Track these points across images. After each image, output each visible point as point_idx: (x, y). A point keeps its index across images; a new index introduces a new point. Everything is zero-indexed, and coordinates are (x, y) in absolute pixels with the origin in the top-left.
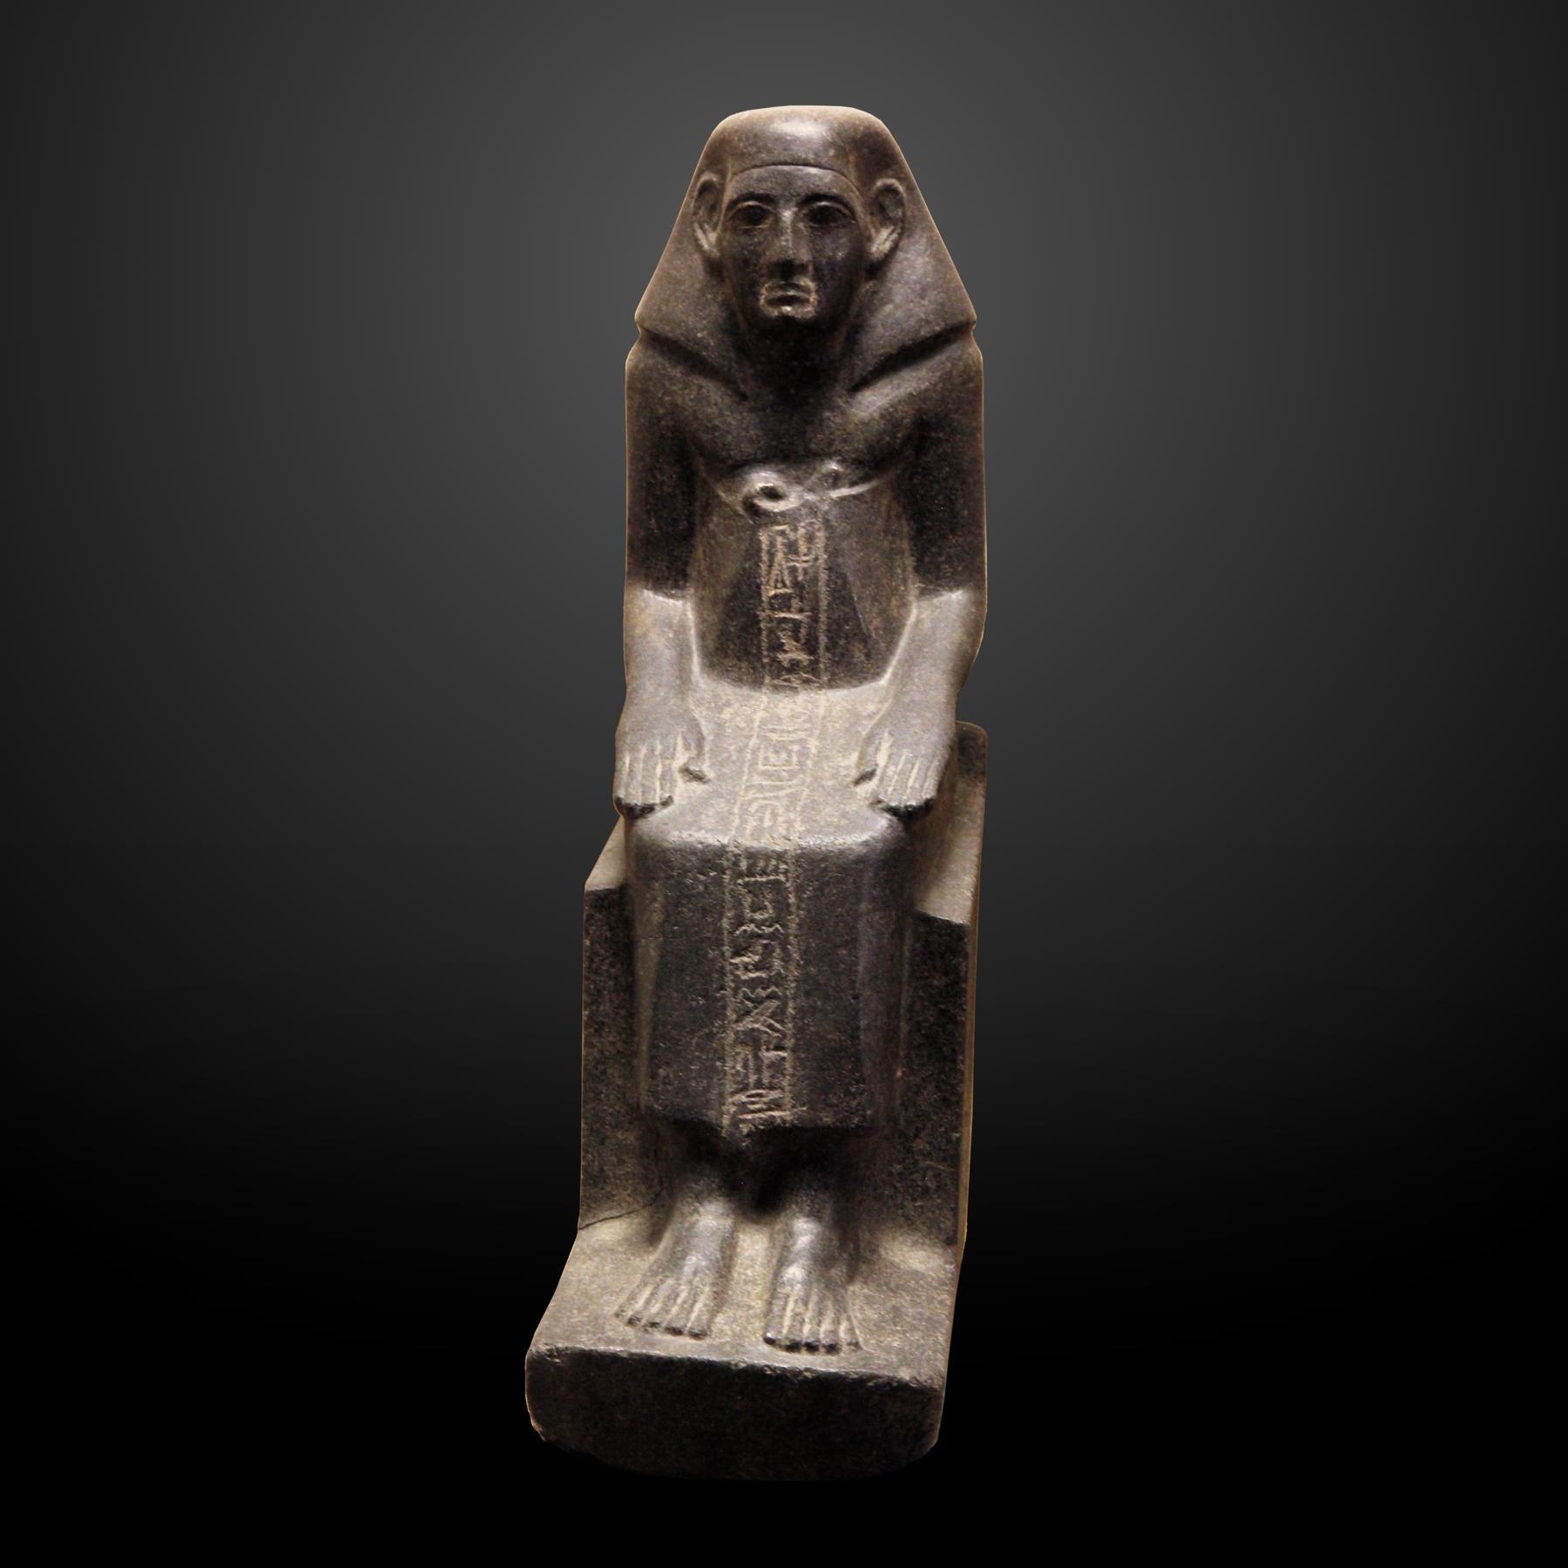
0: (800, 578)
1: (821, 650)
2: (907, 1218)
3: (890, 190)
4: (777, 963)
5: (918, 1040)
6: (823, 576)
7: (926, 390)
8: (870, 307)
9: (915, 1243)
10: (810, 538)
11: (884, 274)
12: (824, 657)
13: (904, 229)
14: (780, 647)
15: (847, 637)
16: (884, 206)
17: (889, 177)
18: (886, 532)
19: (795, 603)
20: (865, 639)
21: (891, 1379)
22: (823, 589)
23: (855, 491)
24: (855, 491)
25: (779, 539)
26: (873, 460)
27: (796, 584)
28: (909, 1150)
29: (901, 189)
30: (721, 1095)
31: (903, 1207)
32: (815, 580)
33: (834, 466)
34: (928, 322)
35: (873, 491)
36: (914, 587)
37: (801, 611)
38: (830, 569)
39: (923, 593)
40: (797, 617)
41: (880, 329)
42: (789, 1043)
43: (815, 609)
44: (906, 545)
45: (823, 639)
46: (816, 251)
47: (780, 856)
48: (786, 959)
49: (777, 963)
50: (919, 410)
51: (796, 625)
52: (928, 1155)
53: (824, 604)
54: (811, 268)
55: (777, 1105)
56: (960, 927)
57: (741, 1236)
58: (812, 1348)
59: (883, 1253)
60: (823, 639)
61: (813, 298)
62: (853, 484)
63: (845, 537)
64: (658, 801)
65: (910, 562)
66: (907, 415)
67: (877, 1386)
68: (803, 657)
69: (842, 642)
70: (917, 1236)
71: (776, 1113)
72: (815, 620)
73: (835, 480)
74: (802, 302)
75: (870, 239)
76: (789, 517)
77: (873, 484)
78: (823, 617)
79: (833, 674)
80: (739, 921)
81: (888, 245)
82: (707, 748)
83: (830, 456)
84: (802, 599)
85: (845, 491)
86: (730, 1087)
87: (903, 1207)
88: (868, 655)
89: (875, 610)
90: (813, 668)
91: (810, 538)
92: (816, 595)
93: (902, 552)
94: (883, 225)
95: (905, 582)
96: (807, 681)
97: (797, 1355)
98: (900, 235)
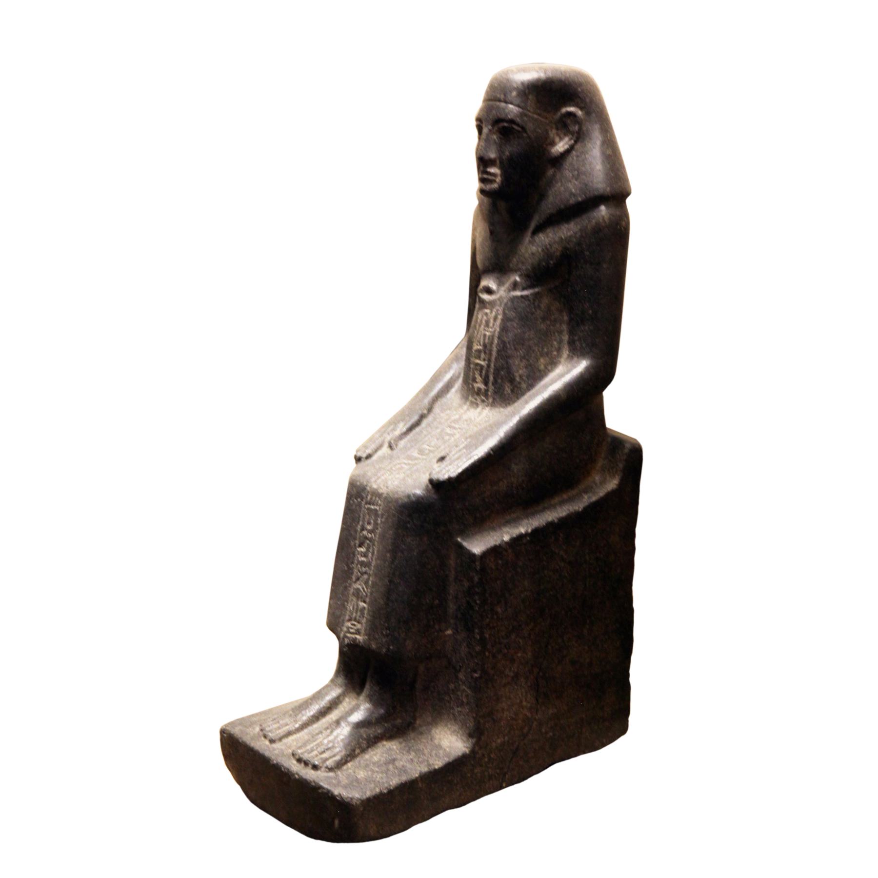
0: (487, 341)
1: (490, 384)
2: (454, 715)
3: (570, 114)
4: (370, 555)
5: (459, 615)
6: (496, 341)
7: (570, 236)
8: (550, 183)
9: (454, 731)
10: (495, 319)
11: (561, 165)
12: (491, 388)
13: (579, 137)
14: (474, 380)
15: (502, 378)
16: (565, 124)
17: (570, 106)
18: (544, 319)
19: (483, 356)
20: (512, 381)
21: (329, 791)
22: (495, 349)
23: (525, 293)
24: (525, 293)
25: (485, 318)
26: (537, 277)
27: (485, 346)
28: (457, 677)
29: (580, 113)
30: (343, 621)
31: (453, 708)
32: (492, 343)
33: (518, 279)
34: (574, 195)
35: (536, 295)
36: (565, 353)
37: (484, 360)
38: (499, 338)
39: (570, 358)
40: (482, 363)
41: (551, 199)
42: (368, 600)
43: (489, 360)
44: (564, 327)
45: (491, 378)
46: (500, 151)
47: (379, 495)
48: (373, 553)
49: (370, 555)
50: (566, 249)
51: (482, 367)
52: (464, 683)
53: (493, 359)
54: (498, 162)
55: (358, 632)
56: (474, 555)
57: (347, 699)
58: (306, 763)
59: (433, 731)
60: (491, 378)
61: (498, 179)
62: (524, 289)
63: (511, 320)
64: (364, 455)
65: (566, 338)
66: (557, 249)
67: (322, 792)
68: (482, 387)
69: (499, 381)
70: (456, 727)
71: (358, 637)
72: (489, 366)
73: (515, 286)
74: (492, 182)
75: (553, 144)
76: (492, 304)
77: (536, 290)
78: (492, 365)
79: (494, 399)
80: (363, 529)
81: (567, 147)
82: (417, 429)
83: (516, 271)
84: (485, 353)
85: (518, 293)
86: (347, 618)
87: (453, 708)
88: (512, 391)
89: (522, 364)
90: (486, 395)
91: (495, 319)
92: (491, 351)
93: (560, 332)
94: (565, 135)
95: (559, 350)
96: (483, 401)
97: (298, 765)
98: (576, 142)
